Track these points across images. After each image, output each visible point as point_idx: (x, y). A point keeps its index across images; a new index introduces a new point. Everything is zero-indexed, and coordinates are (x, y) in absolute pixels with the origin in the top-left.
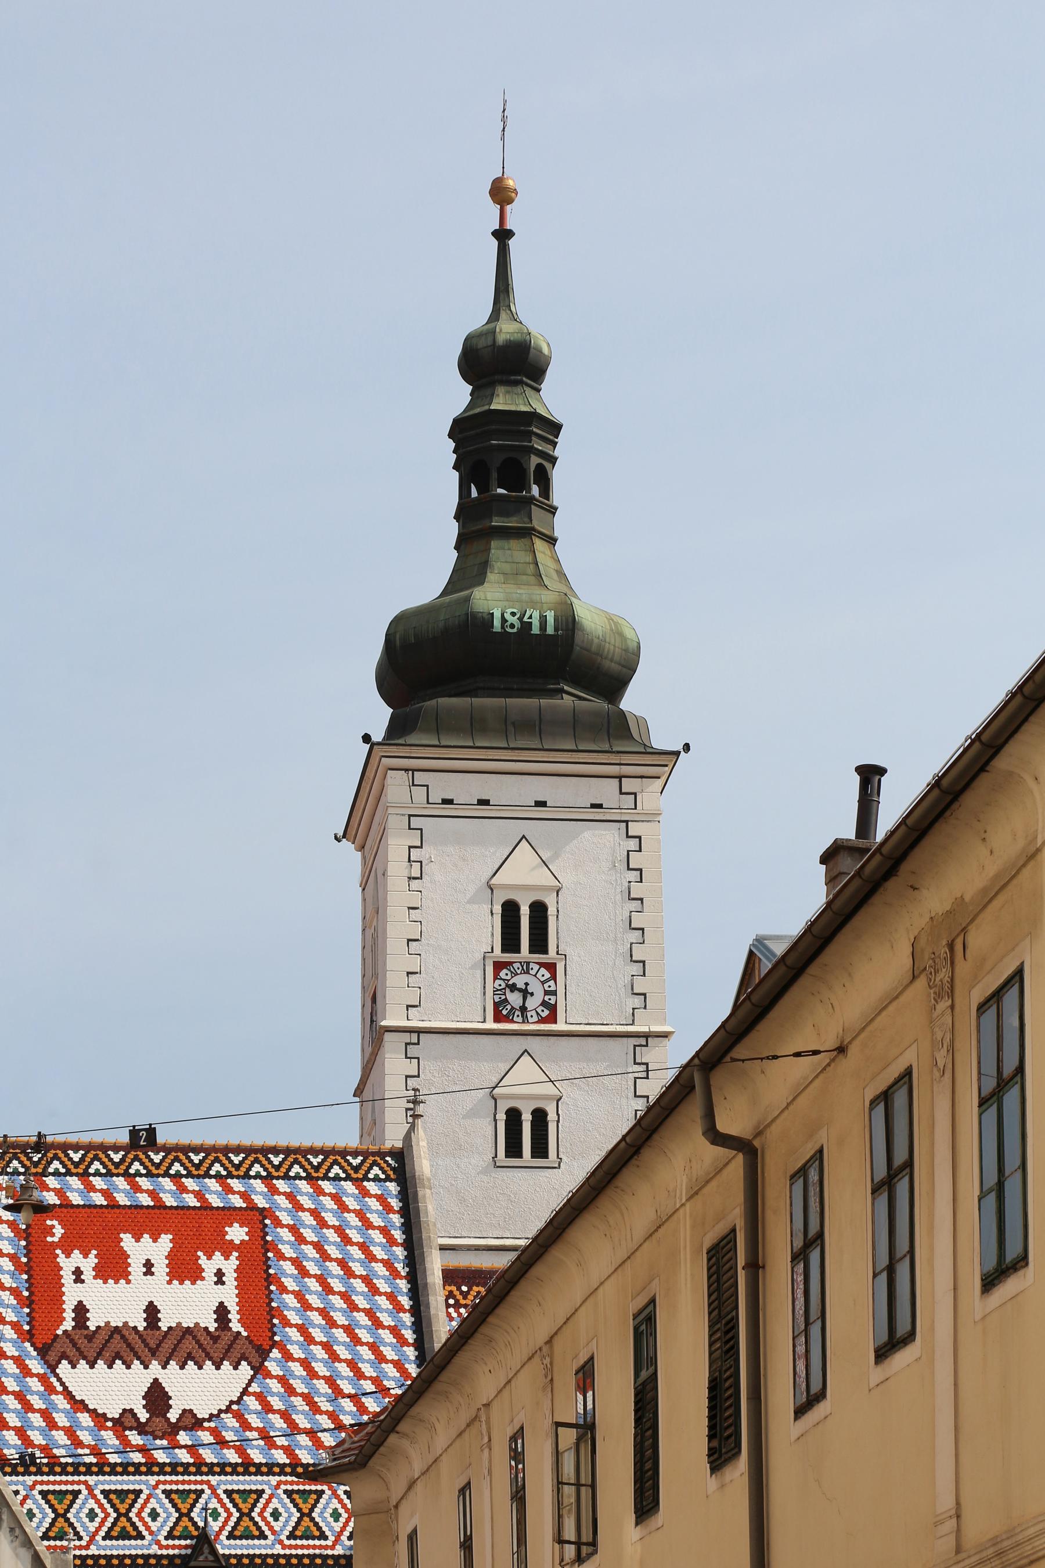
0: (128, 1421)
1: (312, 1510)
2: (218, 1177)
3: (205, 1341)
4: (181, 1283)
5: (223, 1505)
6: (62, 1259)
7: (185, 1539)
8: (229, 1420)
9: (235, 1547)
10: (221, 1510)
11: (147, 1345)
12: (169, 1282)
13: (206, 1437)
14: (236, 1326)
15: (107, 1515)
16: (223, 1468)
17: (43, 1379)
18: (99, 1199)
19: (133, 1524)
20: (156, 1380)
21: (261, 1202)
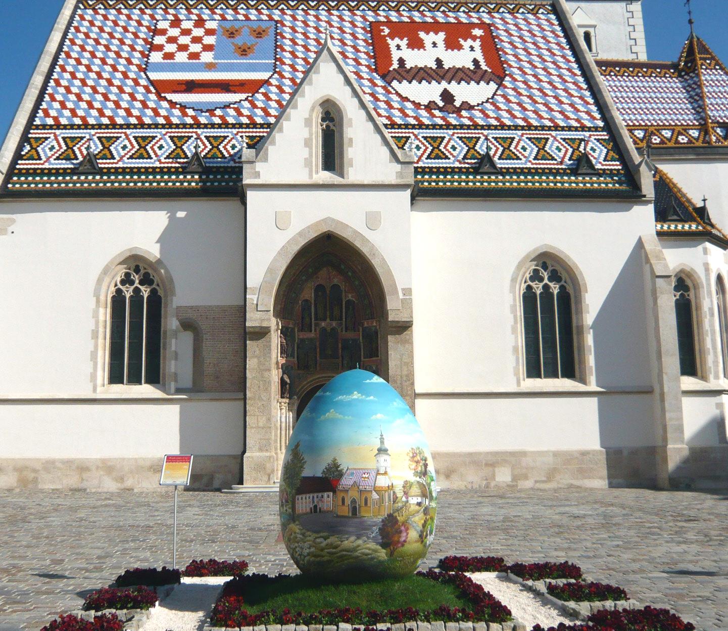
0: (432, 106)
1: (544, 147)
2: (464, 12)
3: (470, 73)
4: (453, 50)
5: (493, 144)
6: (389, 41)
7: (474, 159)
8: (488, 106)
9: (504, 164)
10: (492, 146)
11: (438, 75)
12: (446, 50)
13: (477, 114)
14: (484, 67)
15: (427, 148)
16: (489, 127)
17: (384, 88)
18: (406, 20)
19: (442, 152)
20: (445, 89)
21: (488, 21)
